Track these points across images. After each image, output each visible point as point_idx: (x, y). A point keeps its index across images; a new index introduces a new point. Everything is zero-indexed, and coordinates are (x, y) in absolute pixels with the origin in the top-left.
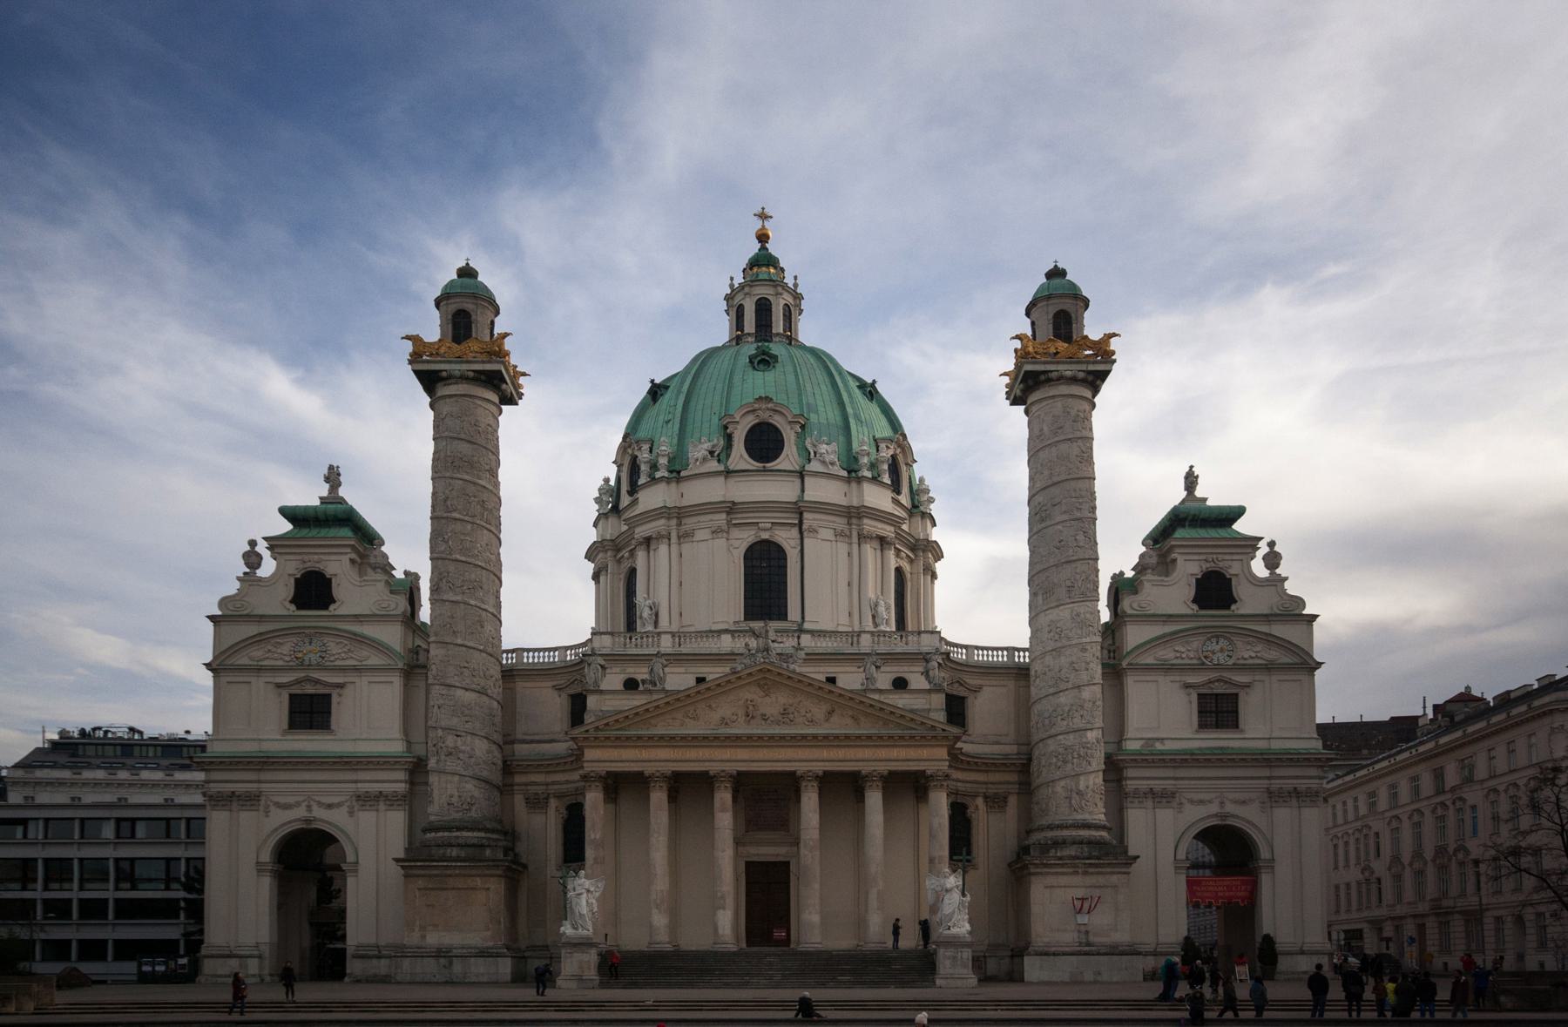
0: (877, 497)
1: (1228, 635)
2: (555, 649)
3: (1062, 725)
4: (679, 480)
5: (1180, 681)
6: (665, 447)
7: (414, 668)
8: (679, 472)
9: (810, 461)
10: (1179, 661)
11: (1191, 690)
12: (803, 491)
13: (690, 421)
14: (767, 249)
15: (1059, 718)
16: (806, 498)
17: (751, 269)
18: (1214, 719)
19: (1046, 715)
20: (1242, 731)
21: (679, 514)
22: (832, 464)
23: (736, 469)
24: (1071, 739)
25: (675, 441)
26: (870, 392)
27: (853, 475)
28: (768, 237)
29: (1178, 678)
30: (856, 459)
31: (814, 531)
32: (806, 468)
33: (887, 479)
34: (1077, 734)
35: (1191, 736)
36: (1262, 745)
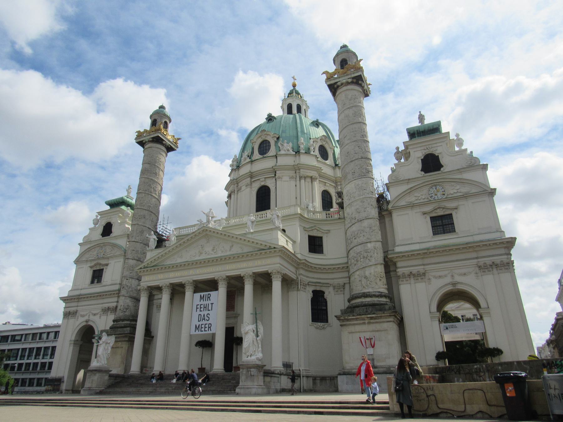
3: (355, 242)
5: (420, 212)
9: (280, 151)
10: (418, 201)
11: (425, 215)
12: (277, 163)
15: (354, 238)
18: (442, 229)
19: (349, 238)
21: (237, 182)
22: (288, 150)
24: (359, 249)
27: (298, 153)
28: (296, 85)
29: (419, 210)
31: (279, 178)
34: (362, 245)
35: (430, 240)
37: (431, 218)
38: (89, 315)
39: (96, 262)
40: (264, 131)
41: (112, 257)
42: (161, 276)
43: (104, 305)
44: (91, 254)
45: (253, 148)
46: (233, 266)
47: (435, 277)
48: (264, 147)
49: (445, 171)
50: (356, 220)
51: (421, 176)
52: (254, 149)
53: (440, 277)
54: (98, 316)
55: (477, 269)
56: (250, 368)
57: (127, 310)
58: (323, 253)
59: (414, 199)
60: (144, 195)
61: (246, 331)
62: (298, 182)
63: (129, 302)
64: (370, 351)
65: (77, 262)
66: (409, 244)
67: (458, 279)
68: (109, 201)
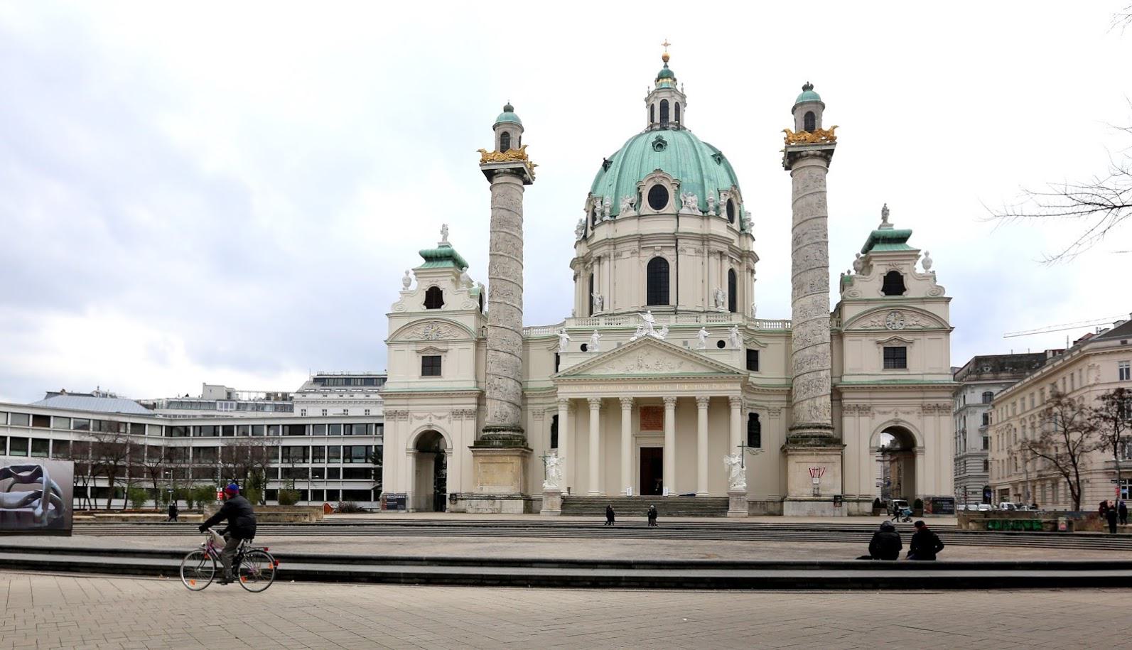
0: (718, 228)
1: (901, 311)
2: (549, 327)
3: (807, 368)
4: (615, 222)
6: (608, 203)
7: (480, 342)
8: (615, 217)
10: (874, 328)
12: (678, 226)
13: (621, 184)
14: (667, 67)
15: (806, 363)
16: (680, 231)
17: (658, 81)
20: (908, 370)
22: (694, 208)
23: (644, 214)
25: (614, 197)
26: (719, 159)
27: (705, 214)
29: (872, 338)
30: (707, 205)
31: (683, 250)
32: (680, 212)
33: (724, 215)
36: (920, 378)
37: (885, 348)
38: (430, 418)
39: (429, 346)
40: (660, 171)
41: (453, 341)
42: (588, 388)
43: (454, 406)
44: (414, 333)
45: (640, 195)
46: (686, 387)
47: (879, 412)
48: (658, 197)
49: (906, 297)
50: (811, 343)
51: (879, 297)
52: (643, 196)
53: (885, 413)
54: (447, 419)
55: (921, 408)
56: (741, 495)
57: (507, 419)
58: (757, 370)
59: (870, 324)
60: (507, 259)
61: (734, 462)
62: (706, 258)
63: (506, 407)
64: (816, 481)
65: (390, 342)
66: (859, 375)
67: (901, 416)
68: (426, 251)
